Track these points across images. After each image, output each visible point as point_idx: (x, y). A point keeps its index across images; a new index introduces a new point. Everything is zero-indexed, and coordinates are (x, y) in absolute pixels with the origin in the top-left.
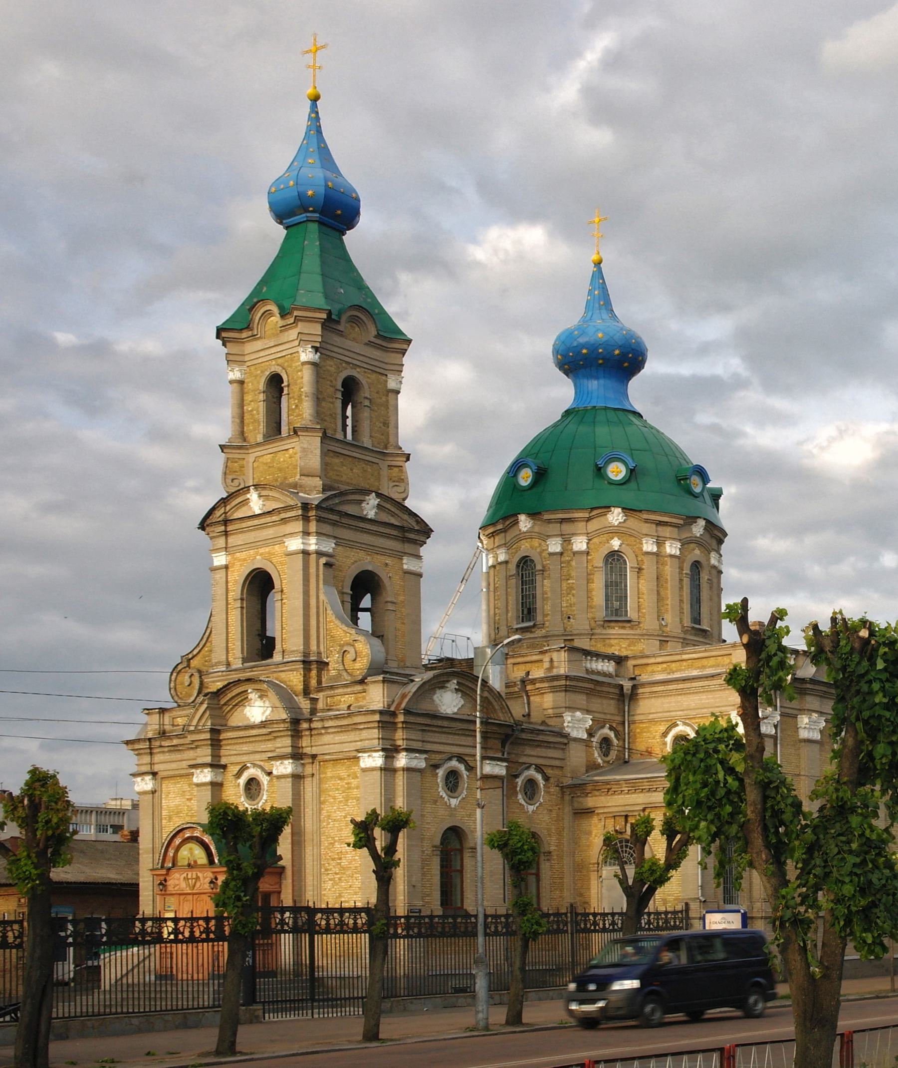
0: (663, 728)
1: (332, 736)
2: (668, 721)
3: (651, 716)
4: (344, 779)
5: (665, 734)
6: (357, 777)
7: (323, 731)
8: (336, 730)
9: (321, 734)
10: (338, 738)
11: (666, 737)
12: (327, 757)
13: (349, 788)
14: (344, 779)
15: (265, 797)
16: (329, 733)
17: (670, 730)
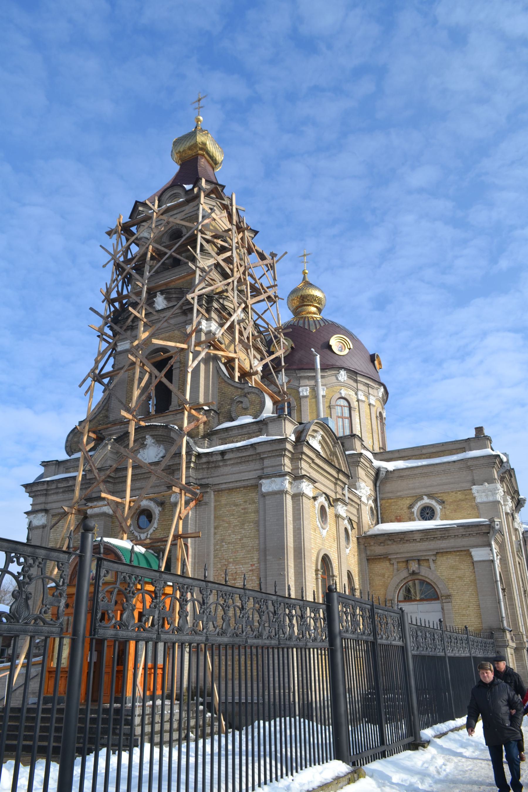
0: (408, 502)
1: (229, 468)
2: (413, 497)
3: (399, 494)
5: (411, 507)
6: (254, 502)
7: (221, 464)
8: (236, 461)
9: (219, 467)
10: (236, 469)
11: (413, 508)
12: (224, 486)
13: (247, 513)
15: (155, 525)
16: (226, 465)
17: (417, 503)
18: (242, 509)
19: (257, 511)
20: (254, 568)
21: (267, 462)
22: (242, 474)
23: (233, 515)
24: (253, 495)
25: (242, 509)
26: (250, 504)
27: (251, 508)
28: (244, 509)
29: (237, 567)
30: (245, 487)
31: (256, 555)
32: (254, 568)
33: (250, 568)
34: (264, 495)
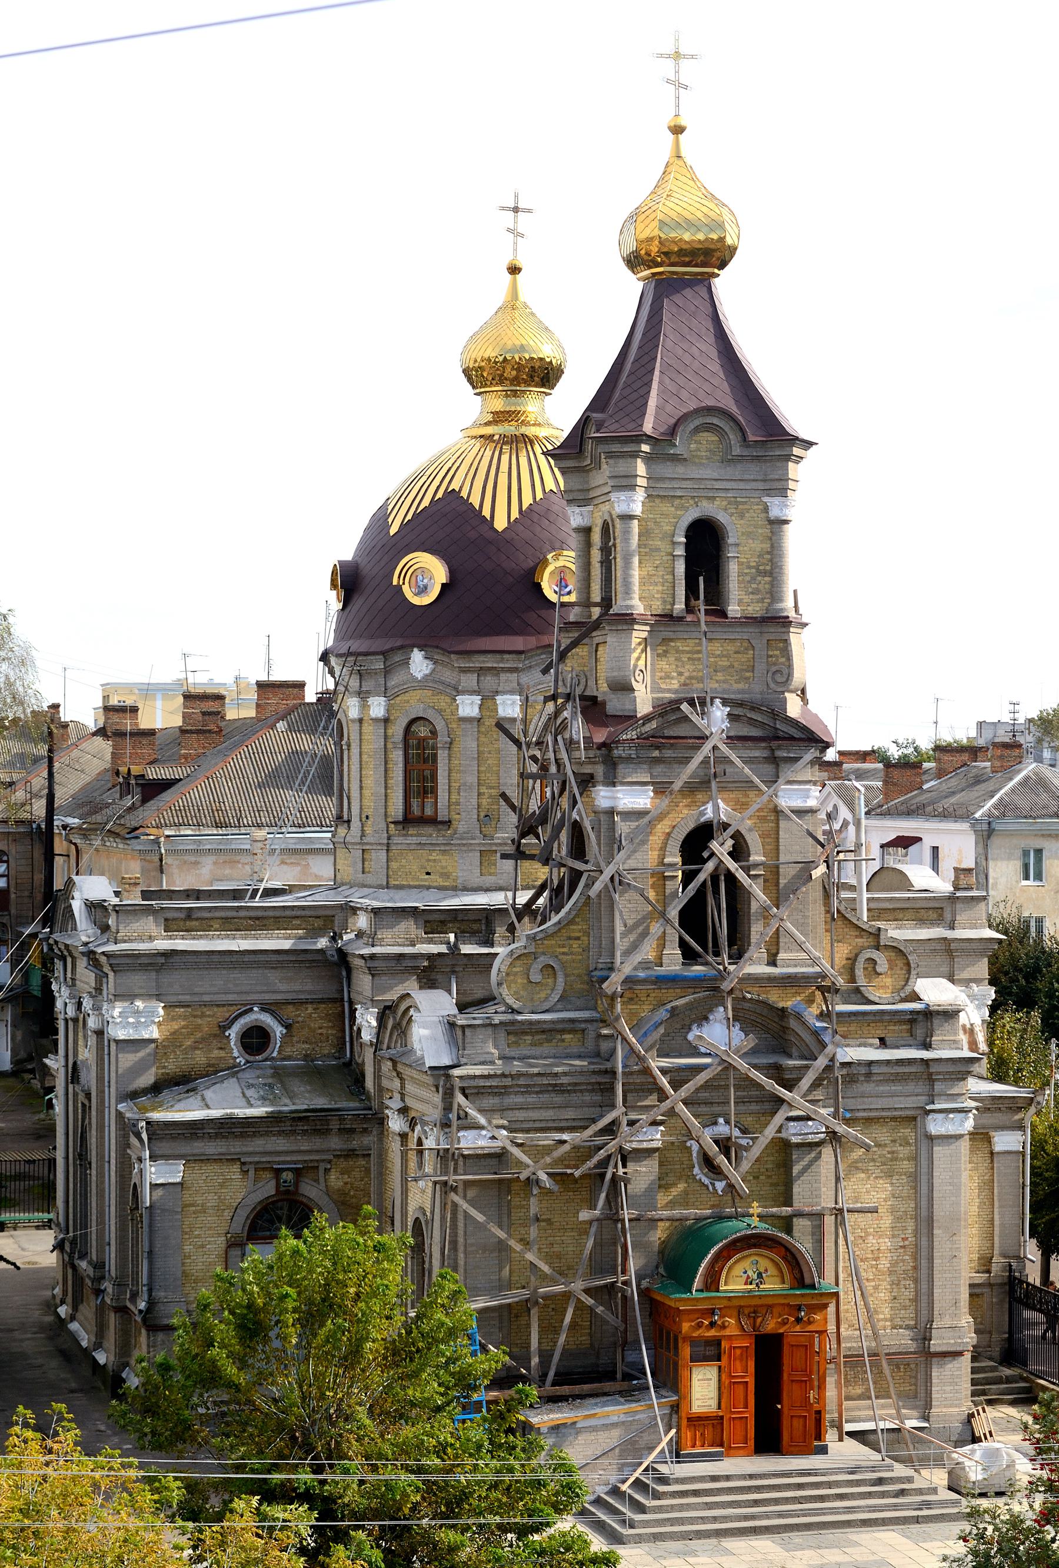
4: (885, 1145)
6: (908, 1144)
13: (896, 1159)
14: (885, 1145)
16: (868, 1082)
18: (889, 1153)
19: (915, 1158)
20: (907, 1243)
21: (938, 1087)
22: (896, 1099)
23: (873, 1160)
24: (907, 1132)
25: (889, 1153)
26: (901, 1145)
27: (904, 1152)
28: (893, 1152)
29: (881, 1240)
30: (894, 1119)
31: (910, 1225)
32: (907, 1243)
33: (901, 1244)
34: (931, 1138)
